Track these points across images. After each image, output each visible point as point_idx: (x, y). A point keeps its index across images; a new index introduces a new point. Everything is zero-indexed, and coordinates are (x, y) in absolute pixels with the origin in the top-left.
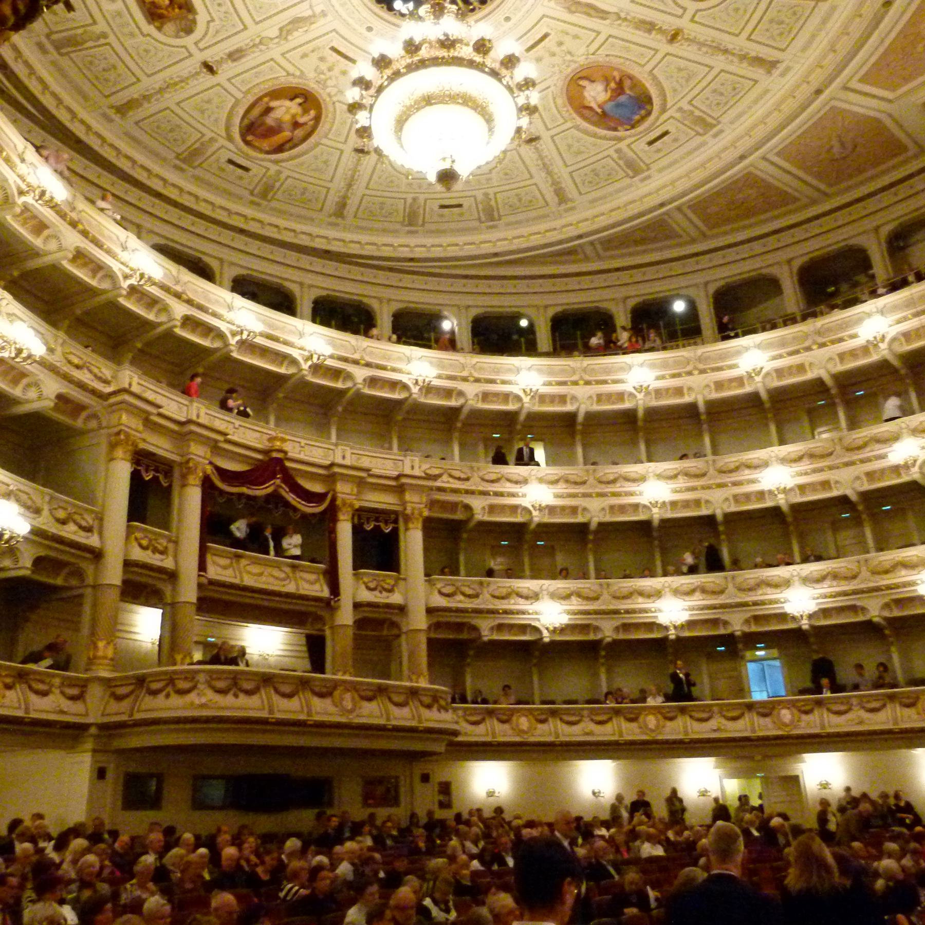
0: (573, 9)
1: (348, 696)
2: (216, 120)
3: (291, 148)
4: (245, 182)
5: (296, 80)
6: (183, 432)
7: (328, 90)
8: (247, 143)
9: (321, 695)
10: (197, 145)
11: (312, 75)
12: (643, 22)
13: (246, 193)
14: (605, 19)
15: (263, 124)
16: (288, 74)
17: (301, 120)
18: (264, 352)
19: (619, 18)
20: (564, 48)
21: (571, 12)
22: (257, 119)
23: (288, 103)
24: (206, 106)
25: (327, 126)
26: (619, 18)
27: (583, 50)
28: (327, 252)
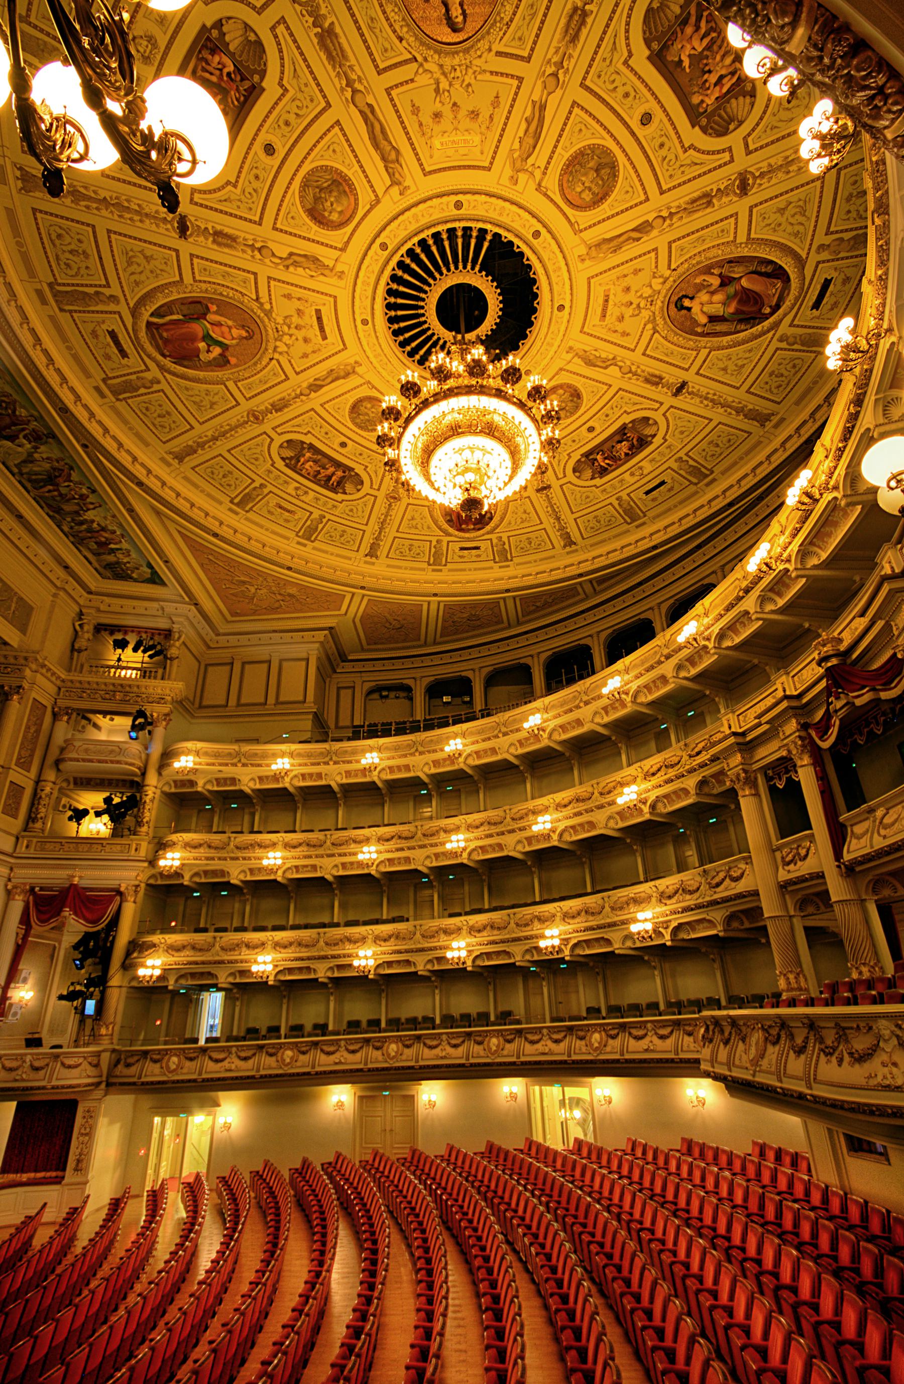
0: (393, 156)
5: (659, 321)
7: (657, 287)
11: (646, 314)
12: (330, 57)
14: (370, 106)
15: (738, 312)
16: (655, 331)
17: (716, 282)
19: (355, 91)
20: (438, 107)
21: (398, 152)
22: (732, 321)
23: (696, 309)
24: (731, 368)
25: (714, 252)
26: (355, 91)
27: (423, 80)
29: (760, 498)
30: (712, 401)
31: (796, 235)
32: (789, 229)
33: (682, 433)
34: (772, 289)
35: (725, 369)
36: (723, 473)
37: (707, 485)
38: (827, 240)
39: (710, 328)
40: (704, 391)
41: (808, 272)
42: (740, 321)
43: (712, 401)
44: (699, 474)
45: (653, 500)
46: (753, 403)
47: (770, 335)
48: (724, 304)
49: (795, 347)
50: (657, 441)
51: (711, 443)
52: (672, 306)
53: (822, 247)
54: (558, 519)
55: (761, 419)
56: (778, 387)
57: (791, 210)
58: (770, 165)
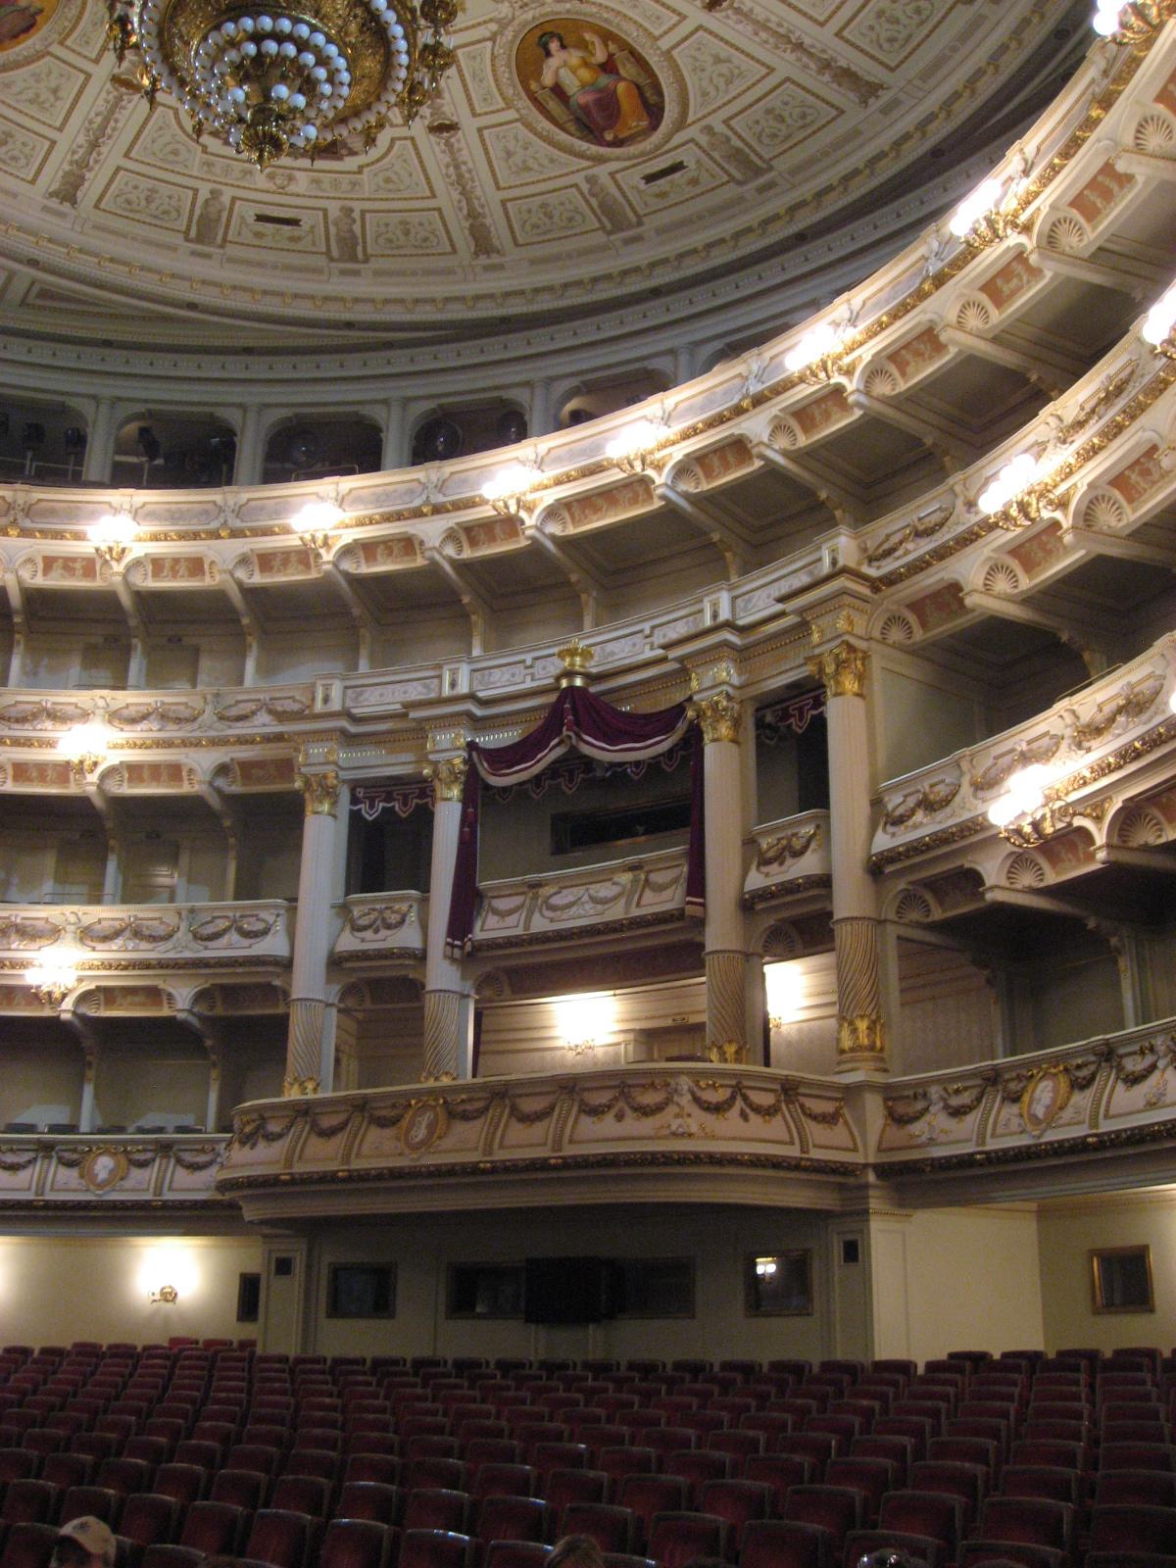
1: (426, 1118)
2: (552, 161)
3: (661, 94)
4: (704, 177)
5: (509, 33)
6: (408, 728)
8: (618, 143)
9: (383, 1123)
10: (594, 202)
13: (731, 191)
15: (585, 108)
16: (493, 38)
17: (600, 56)
18: (608, 496)
23: (553, 63)
24: (517, 159)
28: (936, 153)
29: (389, 345)
30: (460, 176)
31: (705, 94)
32: (705, 83)
33: (388, 180)
34: (636, 122)
35: (509, 154)
36: (377, 273)
37: (343, 272)
38: (720, 128)
39: (541, 95)
40: (464, 155)
41: (677, 139)
42: (578, 120)
43: (460, 176)
44: (349, 249)
45: (258, 235)
46: (495, 220)
47: (586, 163)
48: (583, 86)
49: (594, 202)
50: (350, 163)
51: (404, 223)
52: (538, 33)
53: (709, 130)
54: (94, 145)
55: (483, 243)
56: (535, 226)
57: (724, 68)
58: (751, 10)
